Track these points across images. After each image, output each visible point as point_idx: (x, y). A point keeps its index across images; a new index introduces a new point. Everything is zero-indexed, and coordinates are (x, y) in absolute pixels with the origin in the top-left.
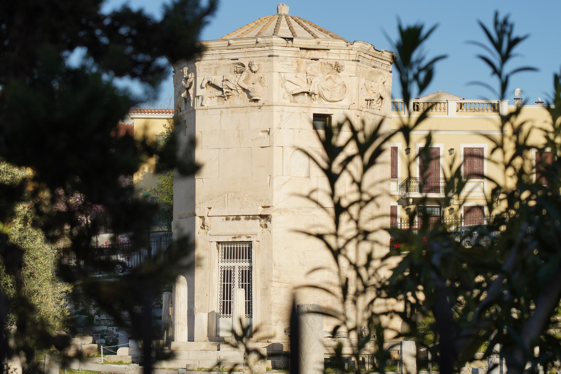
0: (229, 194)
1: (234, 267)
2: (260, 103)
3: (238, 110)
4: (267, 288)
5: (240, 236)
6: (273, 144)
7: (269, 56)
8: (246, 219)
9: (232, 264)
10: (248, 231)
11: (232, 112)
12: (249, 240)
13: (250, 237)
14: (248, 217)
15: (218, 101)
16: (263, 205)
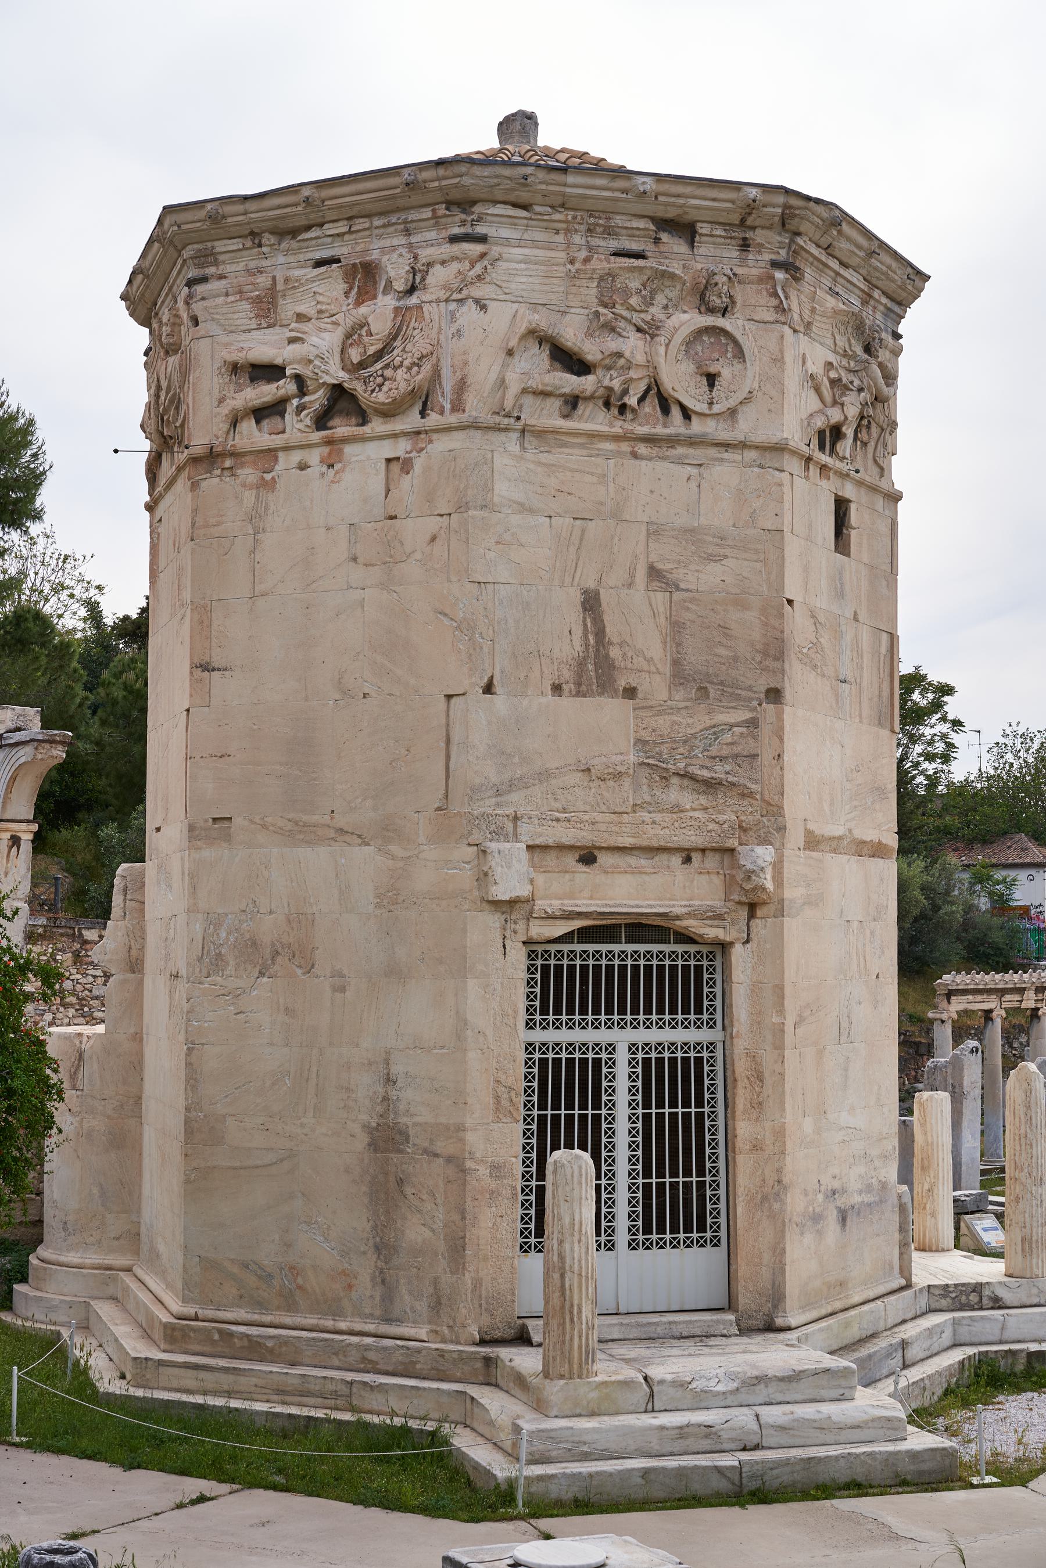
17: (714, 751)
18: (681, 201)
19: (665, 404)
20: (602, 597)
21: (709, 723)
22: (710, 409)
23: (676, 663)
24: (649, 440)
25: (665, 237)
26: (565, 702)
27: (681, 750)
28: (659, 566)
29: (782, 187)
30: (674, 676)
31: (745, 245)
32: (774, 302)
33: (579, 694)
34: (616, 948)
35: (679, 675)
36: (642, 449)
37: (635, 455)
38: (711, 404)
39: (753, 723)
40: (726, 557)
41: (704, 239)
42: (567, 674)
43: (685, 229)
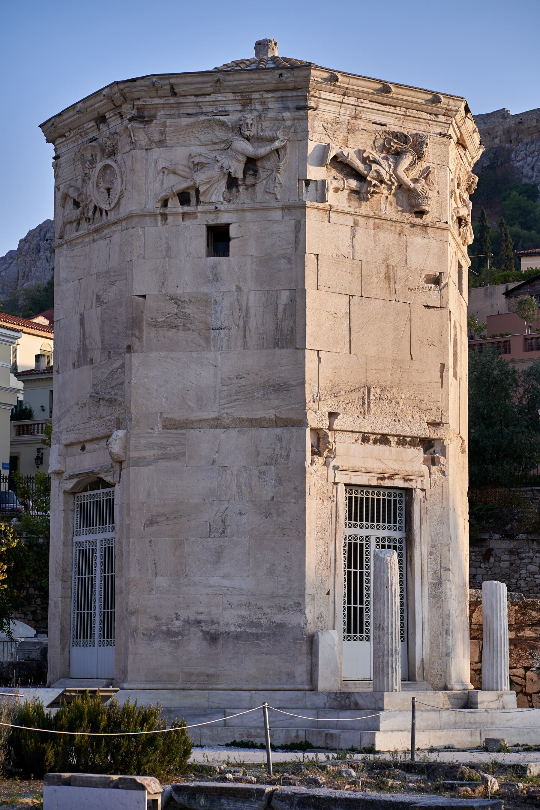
0: (372, 390)
1: (368, 538)
2: (427, 219)
3: (387, 224)
4: (440, 583)
5: (391, 477)
6: (447, 303)
7: (441, 134)
8: (399, 443)
9: (364, 532)
10: (407, 468)
11: (376, 227)
12: (406, 485)
13: (410, 480)
14: (402, 441)
15: (349, 200)
16: (432, 418)
17: (112, 385)
18: (93, 107)
19: (101, 210)
20: (85, 316)
21: (111, 369)
22: (110, 207)
23: (103, 341)
24: (96, 231)
25: (101, 126)
26: (76, 370)
27: (104, 386)
28: (99, 294)
29: (114, 82)
30: (102, 348)
31: (121, 116)
32: (130, 139)
33: (79, 366)
34: (98, 491)
35: (103, 348)
36: (96, 236)
37: (94, 241)
38: (110, 204)
39: (123, 366)
40: (116, 281)
41: (110, 120)
42: (76, 357)
43: (102, 119)
